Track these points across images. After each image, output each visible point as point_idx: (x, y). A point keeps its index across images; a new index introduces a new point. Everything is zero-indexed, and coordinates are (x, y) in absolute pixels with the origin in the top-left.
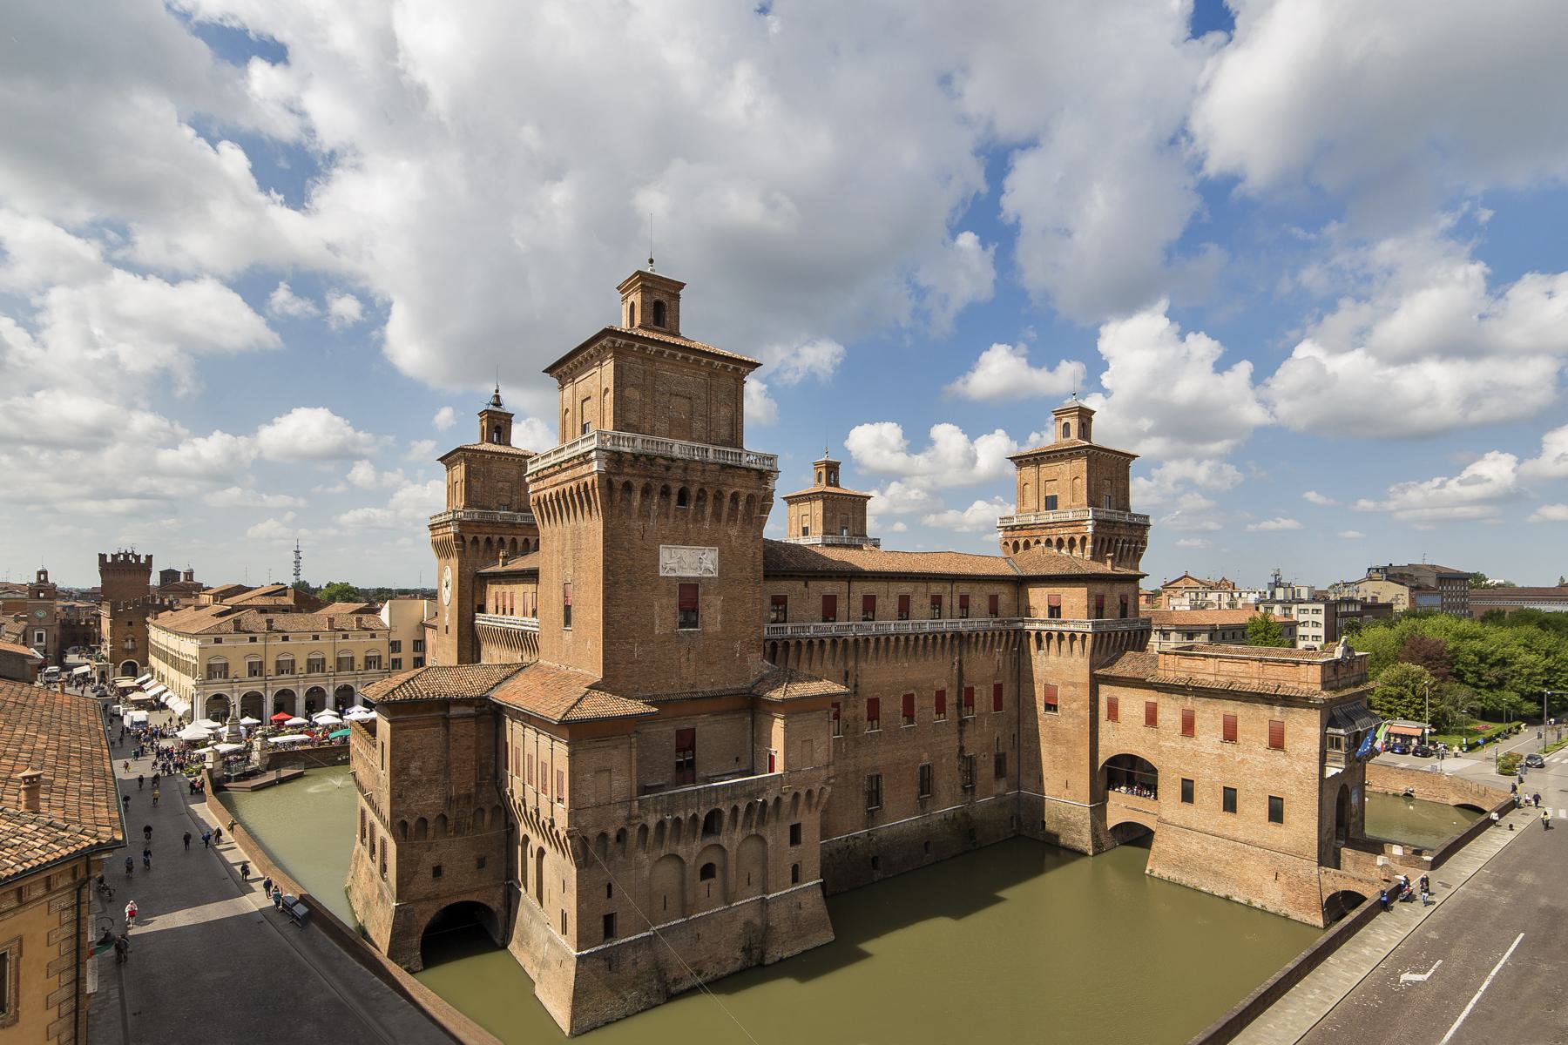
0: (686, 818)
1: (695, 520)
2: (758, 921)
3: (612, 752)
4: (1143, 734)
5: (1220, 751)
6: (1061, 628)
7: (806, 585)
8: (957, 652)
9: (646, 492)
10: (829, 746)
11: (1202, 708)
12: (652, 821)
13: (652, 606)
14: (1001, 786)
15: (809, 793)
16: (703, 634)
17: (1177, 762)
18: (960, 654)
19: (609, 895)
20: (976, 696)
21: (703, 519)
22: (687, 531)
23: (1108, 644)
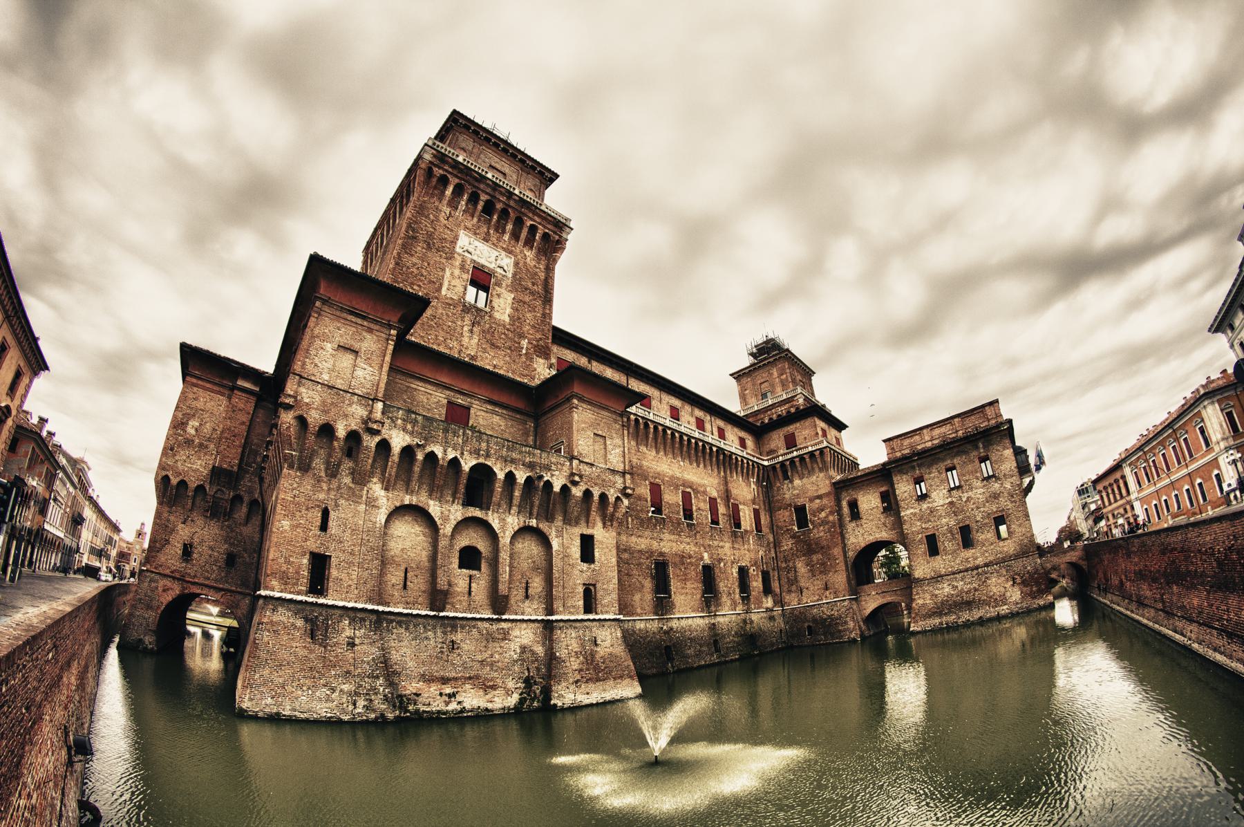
0: (443, 459)
1: (496, 230)
2: (540, 650)
3: (365, 334)
4: (883, 520)
5: (950, 500)
6: (801, 452)
7: (589, 362)
8: (722, 469)
9: (459, 190)
10: (624, 452)
11: (928, 471)
12: (398, 440)
13: (443, 270)
14: (769, 603)
15: (603, 497)
16: (490, 316)
17: (919, 524)
18: (725, 472)
19: (324, 527)
20: (741, 514)
21: (504, 232)
22: (488, 233)
23: (838, 464)
